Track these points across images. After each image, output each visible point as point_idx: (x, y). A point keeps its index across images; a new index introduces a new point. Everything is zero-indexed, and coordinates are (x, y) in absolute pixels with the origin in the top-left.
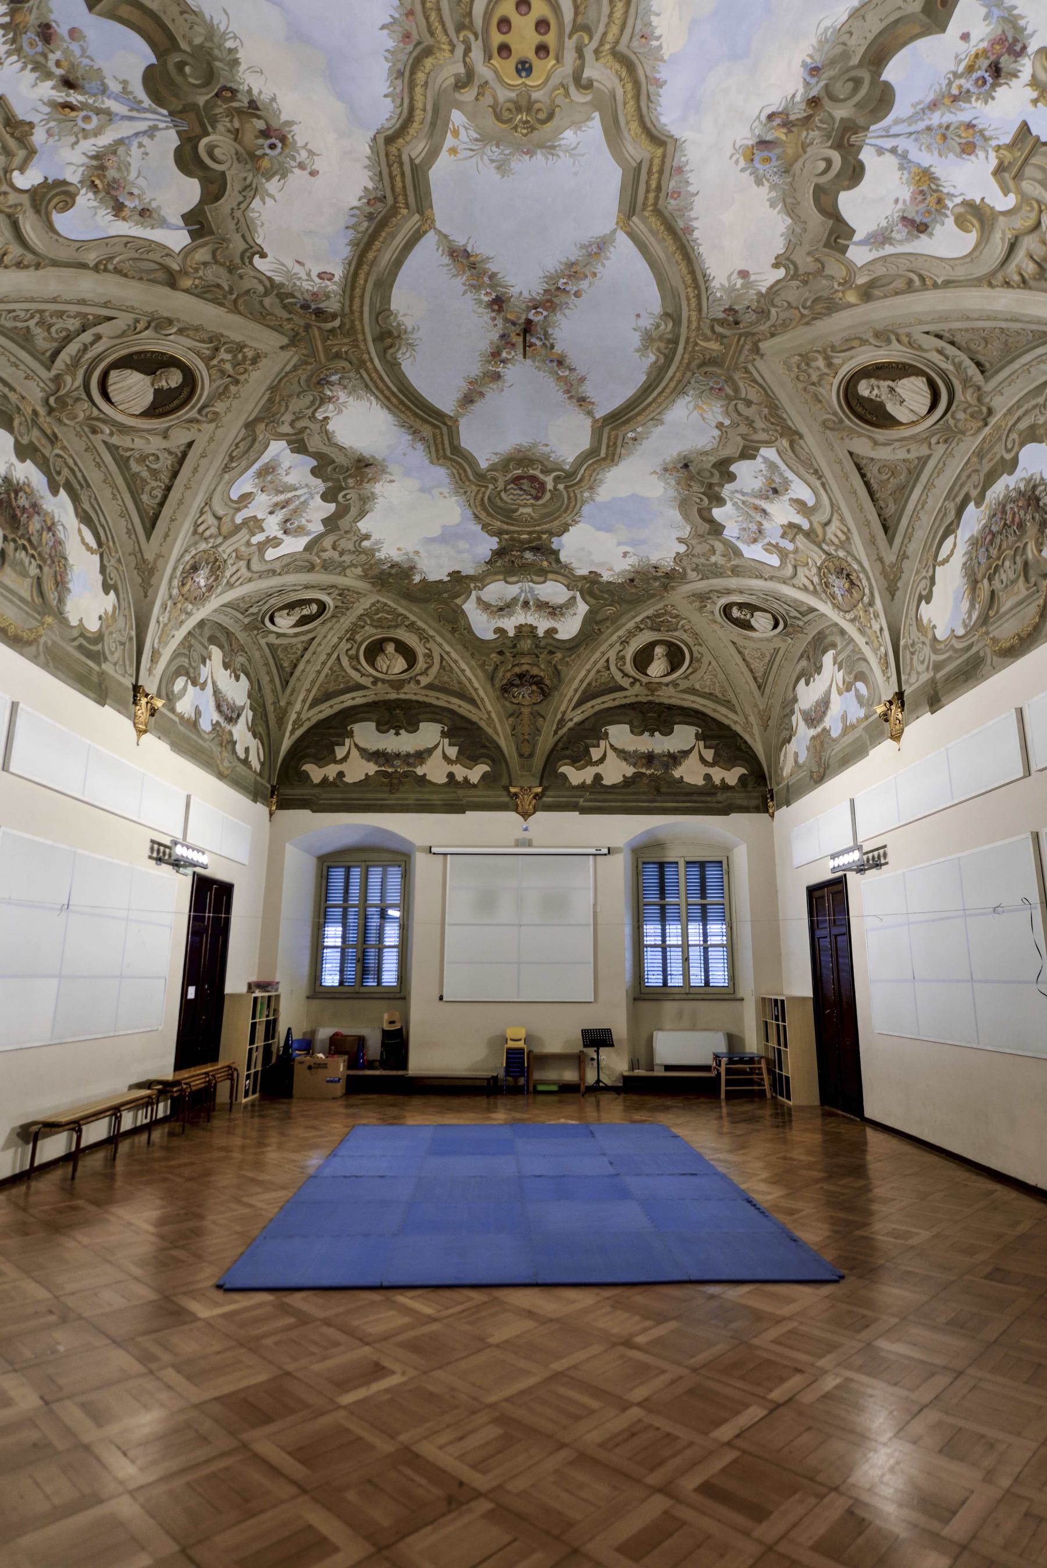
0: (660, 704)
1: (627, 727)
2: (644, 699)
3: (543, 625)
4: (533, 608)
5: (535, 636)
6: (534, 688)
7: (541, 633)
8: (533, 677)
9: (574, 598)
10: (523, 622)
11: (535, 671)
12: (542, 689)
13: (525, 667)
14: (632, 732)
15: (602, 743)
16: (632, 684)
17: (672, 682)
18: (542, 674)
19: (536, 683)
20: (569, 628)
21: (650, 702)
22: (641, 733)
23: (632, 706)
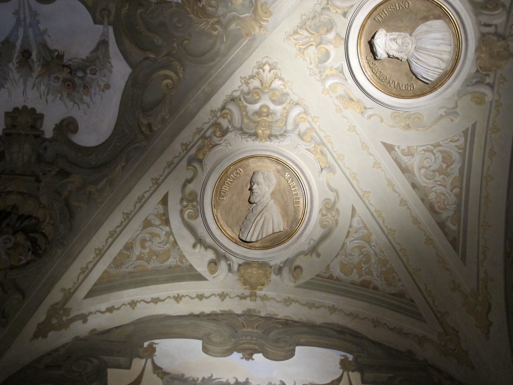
0: (269, 318)
1: (198, 344)
2: (238, 307)
3: (53, 111)
4: (37, 69)
5: (39, 136)
6: (20, 238)
7: (48, 129)
8: (22, 218)
9: (103, 43)
10: (19, 103)
11: (28, 207)
12: (34, 242)
13: (12, 200)
14: (205, 350)
15: (138, 364)
16: (213, 264)
17: (288, 262)
18: (40, 214)
19: (25, 231)
20: (97, 121)
21: (249, 314)
22: (228, 353)
23: (212, 317)
